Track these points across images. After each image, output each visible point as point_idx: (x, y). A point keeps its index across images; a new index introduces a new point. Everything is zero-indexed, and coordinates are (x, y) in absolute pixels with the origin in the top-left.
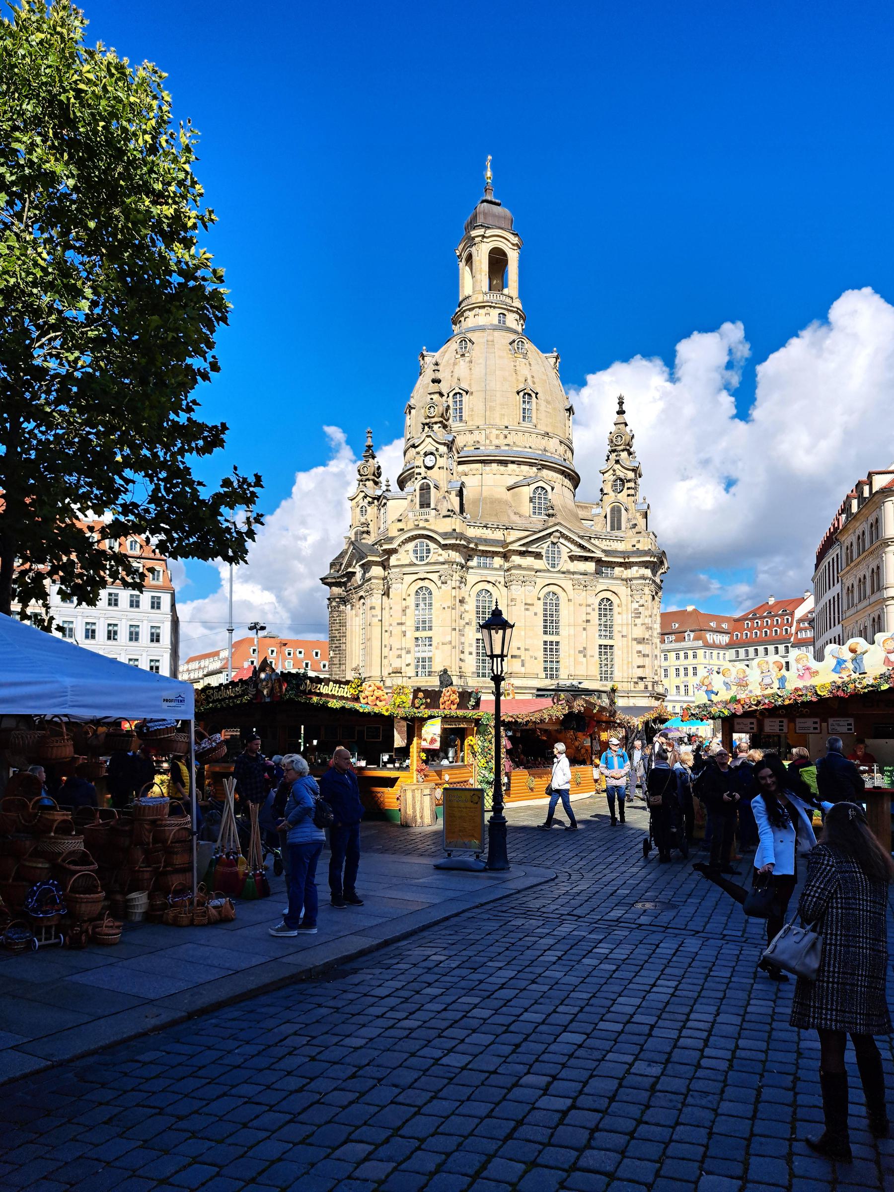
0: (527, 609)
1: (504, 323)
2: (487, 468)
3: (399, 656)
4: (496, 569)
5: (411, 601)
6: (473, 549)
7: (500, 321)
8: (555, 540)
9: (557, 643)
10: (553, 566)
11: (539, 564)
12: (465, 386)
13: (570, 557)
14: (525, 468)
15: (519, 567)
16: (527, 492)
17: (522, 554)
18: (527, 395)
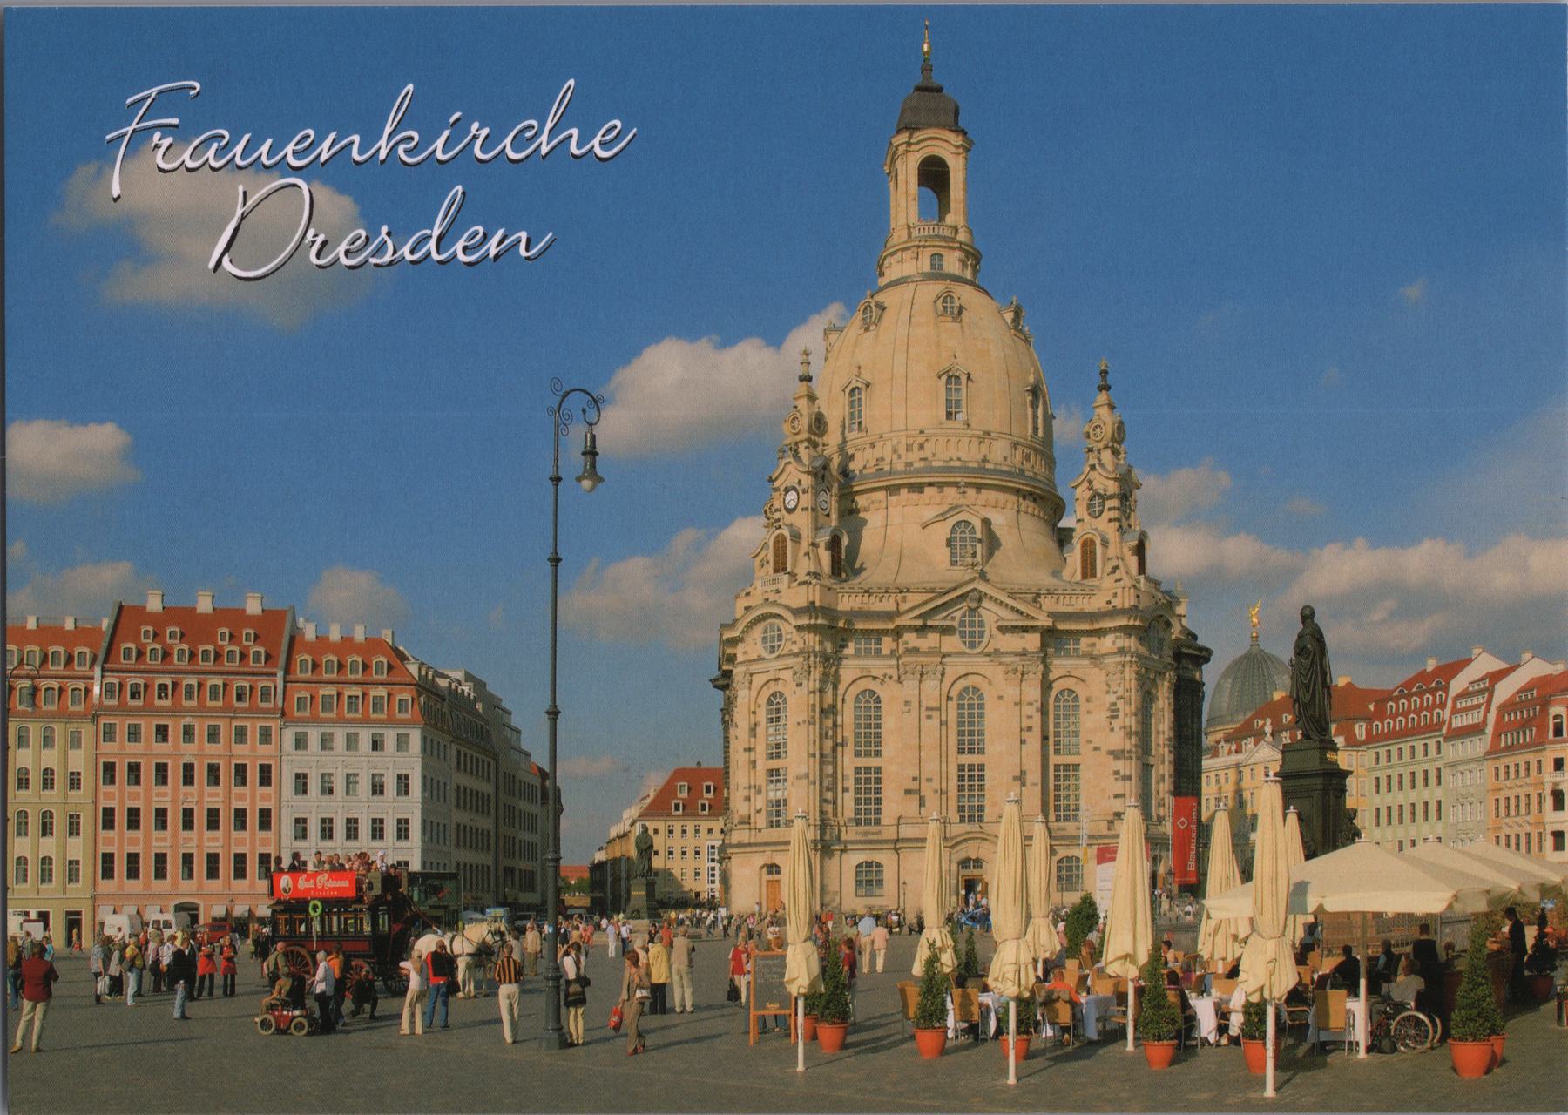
0: (929, 717)
1: (941, 267)
2: (893, 499)
3: (748, 799)
4: (885, 656)
5: (762, 716)
6: (844, 630)
7: (933, 266)
8: (974, 605)
9: (981, 767)
10: (972, 645)
11: (952, 643)
12: (866, 376)
13: (1000, 628)
14: (951, 492)
15: (916, 651)
16: (943, 530)
17: (922, 630)
18: (952, 378)
